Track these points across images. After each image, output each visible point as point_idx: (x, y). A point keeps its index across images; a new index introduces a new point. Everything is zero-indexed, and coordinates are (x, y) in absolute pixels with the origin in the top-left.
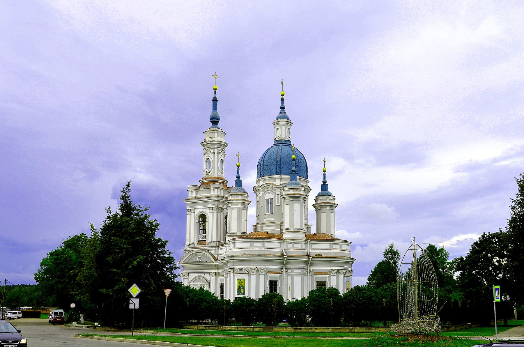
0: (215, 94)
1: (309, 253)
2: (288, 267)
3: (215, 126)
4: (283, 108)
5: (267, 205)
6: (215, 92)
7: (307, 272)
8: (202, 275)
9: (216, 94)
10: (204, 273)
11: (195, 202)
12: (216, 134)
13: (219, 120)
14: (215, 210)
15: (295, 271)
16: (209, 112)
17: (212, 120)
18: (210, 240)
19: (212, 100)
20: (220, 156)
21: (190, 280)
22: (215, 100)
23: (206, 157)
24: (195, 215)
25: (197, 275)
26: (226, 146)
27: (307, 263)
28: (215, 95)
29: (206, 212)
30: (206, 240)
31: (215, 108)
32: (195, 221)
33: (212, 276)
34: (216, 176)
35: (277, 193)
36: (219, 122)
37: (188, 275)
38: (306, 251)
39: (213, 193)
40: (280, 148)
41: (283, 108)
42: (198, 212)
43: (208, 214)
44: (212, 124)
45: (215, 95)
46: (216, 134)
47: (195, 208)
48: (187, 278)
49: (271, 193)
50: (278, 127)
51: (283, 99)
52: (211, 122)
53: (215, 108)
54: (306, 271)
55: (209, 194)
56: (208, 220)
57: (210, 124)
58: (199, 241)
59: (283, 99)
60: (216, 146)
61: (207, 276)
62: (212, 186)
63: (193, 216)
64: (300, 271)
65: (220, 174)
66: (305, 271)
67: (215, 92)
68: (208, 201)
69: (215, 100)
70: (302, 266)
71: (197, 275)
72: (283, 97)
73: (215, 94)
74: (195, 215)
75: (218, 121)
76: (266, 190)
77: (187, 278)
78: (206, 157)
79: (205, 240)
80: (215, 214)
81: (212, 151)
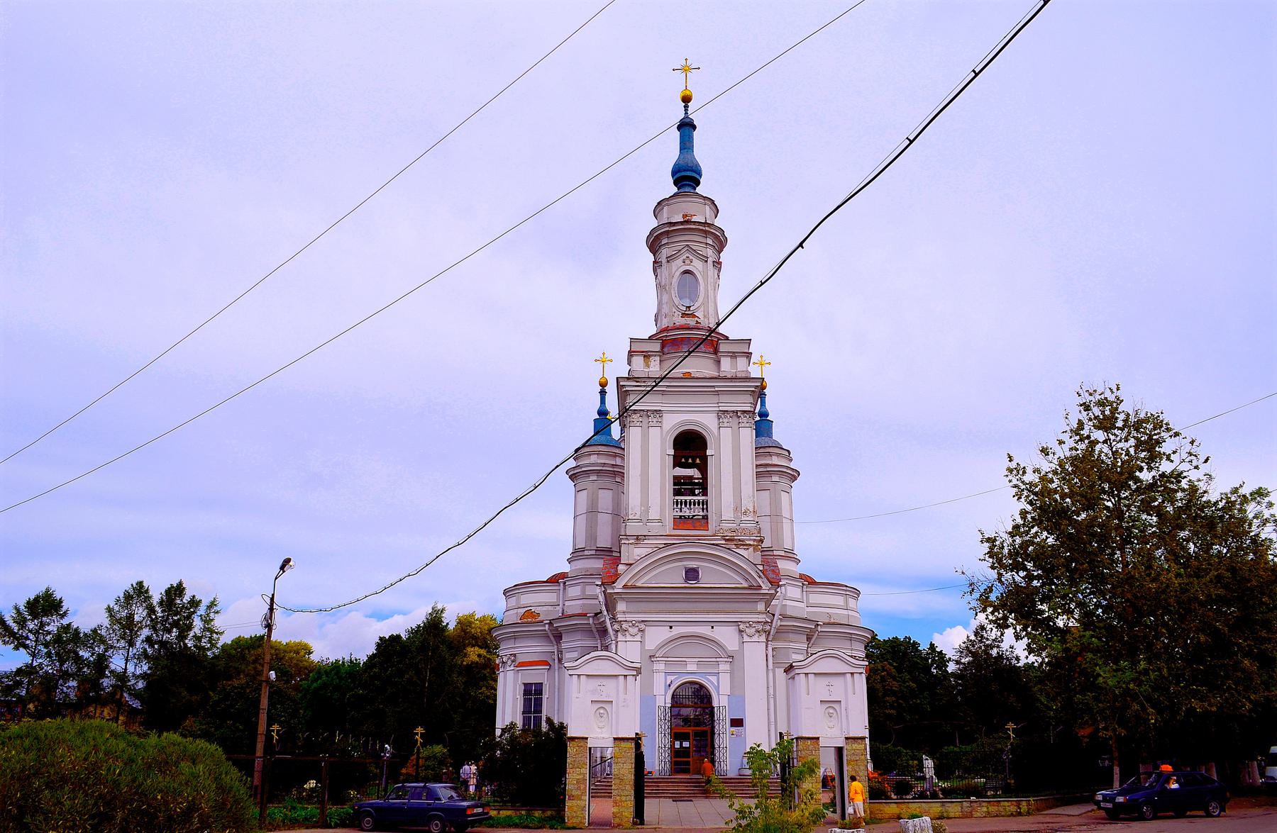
8: (704, 630)
10: (713, 624)
13: (700, 174)
16: (670, 152)
17: (679, 175)
18: (728, 514)
22: (686, 126)
24: (664, 433)
29: (705, 421)
31: (686, 144)
32: (663, 450)
33: (745, 636)
42: (674, 422)
45: (686, 113)
48: (638, 638)
53: (686, 144)
61: (727, 637)
68: (717, 389)
69: (686, 126)
71: (678, 630)
74: (664, 433)
77: (638, 638)
78: (678, 266)
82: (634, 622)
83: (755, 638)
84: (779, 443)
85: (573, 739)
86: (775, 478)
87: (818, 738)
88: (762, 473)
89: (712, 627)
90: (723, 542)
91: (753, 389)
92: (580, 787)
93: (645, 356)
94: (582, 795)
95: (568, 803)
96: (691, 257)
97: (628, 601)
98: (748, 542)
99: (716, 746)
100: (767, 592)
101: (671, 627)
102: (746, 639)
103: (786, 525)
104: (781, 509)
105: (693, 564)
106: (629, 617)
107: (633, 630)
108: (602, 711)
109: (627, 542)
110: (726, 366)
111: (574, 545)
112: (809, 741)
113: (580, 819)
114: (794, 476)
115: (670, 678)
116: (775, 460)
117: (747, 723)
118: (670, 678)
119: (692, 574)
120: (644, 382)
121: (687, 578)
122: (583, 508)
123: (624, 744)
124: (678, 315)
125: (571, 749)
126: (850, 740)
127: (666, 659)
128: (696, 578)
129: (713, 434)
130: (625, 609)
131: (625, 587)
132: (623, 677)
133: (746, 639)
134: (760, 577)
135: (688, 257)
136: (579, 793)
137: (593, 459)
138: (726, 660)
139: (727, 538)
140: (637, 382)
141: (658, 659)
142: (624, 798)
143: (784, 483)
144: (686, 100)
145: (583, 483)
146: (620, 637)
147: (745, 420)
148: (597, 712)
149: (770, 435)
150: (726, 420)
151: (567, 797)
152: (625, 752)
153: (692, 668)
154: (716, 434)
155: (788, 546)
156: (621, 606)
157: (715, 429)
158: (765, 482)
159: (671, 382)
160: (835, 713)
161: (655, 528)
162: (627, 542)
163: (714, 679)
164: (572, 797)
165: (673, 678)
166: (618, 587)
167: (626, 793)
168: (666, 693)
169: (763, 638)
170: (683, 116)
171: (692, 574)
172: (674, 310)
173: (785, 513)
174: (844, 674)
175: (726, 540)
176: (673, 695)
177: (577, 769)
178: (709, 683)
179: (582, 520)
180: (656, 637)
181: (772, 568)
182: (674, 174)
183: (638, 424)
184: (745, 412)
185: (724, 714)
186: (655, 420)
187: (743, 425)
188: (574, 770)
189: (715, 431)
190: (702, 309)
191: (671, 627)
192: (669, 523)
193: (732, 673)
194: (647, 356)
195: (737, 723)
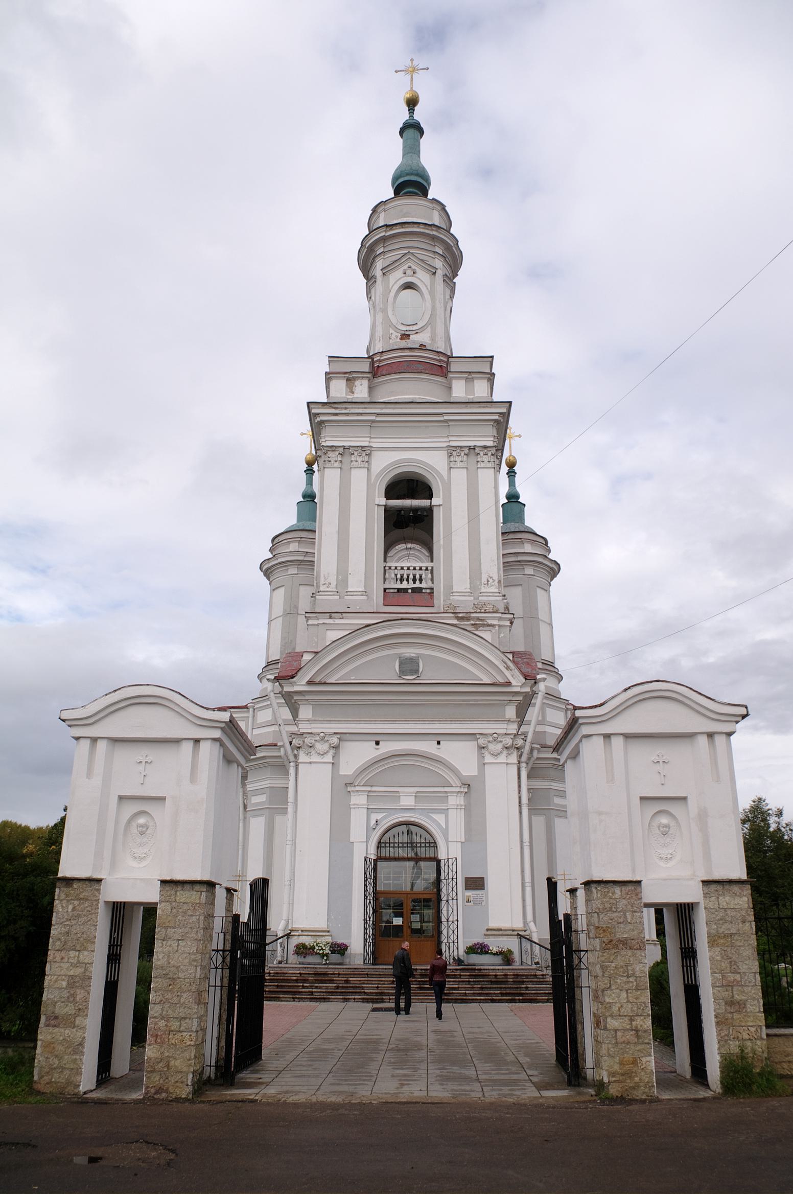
11: (373, 418)
18: (461, 583)
21: (348, 768)
24: (373, 477)
31: (412, 150)
37: (336, 748)
43: (444, 473)
48: (329, 758)
53: (412, 150)
63: (359, 477)
68: (446, 417)
71: (387, 747)
82: (322, 735)
83: (502, 758)
84: (533, 530)
85: (69, 881)
86: (529, 571)
87: (639, 883)
88: (511, 564)
89: (439, 743)
90: (455, 622)
91: (496, 417)
92: (73, 995)
93: (348, 380)
94: (76, 1016)
95: (44, 1034)
96: (414, 267)
97: (316, 706)
98: (490, 622)
99: (443, 919)
100: (518, 689)
101: (377, 743)
102: (488, 759)
103: (543, 628)
104: (537, 609)
105: (410, 652)
106: (317, 728)
107: (321, 747)
108: (142, 820)
109: (316, 622)
110: (459, 390)
111: (267, 657)
112: (617, 890)
113: (67, 1073)
114: (554, 570)
115: (375, 817)
116: (528, 548)
117: (490, 883)
118: (375, 817)
119: (409, 666)
120: (346, 408)
121: (403, 672)
122: (279, 610)
123: (183, 896)
124: (397, 337)
125: (62, 907)
126: (713, 887)
127: (369, 789)
128: (416, 671)
129: (441, 477)
130: (310, 717)
131: (310, 683)
132: (191, 744)
133: (488, 759)
134: (508, 668)
135: (410, 267)
136: (70, 1009)
137: (294, 547)
138: (458, 789)
139: (460, 615)
140: (336, 408)
141: (357, 788)
142: (174, 1025)
143: (541, 579)
145: (280, 576)
146: (302, 757)
147: (485, 458)
148: (134, 824)
149: (521, 518)
150: (458, 459)
151: (43, 1019)
152: (185, 913)
153: (407, 801)
154: (446, 478)
155: (546, 656)
156: (305, 712)
157: (443, 470)
158: (515, 576)
159: (382, 408)
160: (672, 824)
161: (357, 601)
162: (316, 622)
163: (440, 818)
164: (56, 1020)
165: (379, 816)
166: (300, 684)
167: (180, 1012)
168: (367, 842)
169: (514, 759)
171: (409, 666)
172: (391, 331)
173: (542, 615)
174: (691, 736)
175: (459, 619)
176: (380, 842)
177: (72, 954)
178: (434, 823)
179: (278, 624)
181: (525, 660)
183: (336, 464)
184: (485, 447)
185: (454, 870)
186: (360, 459)
187: (482, 465)
188: (63, 954)
189: (444, 473)
190: (429, 329)
191: (377, 743)
192: (378, 596)
193: (468, 809)
194: (350, 379)
195: (476, 883)
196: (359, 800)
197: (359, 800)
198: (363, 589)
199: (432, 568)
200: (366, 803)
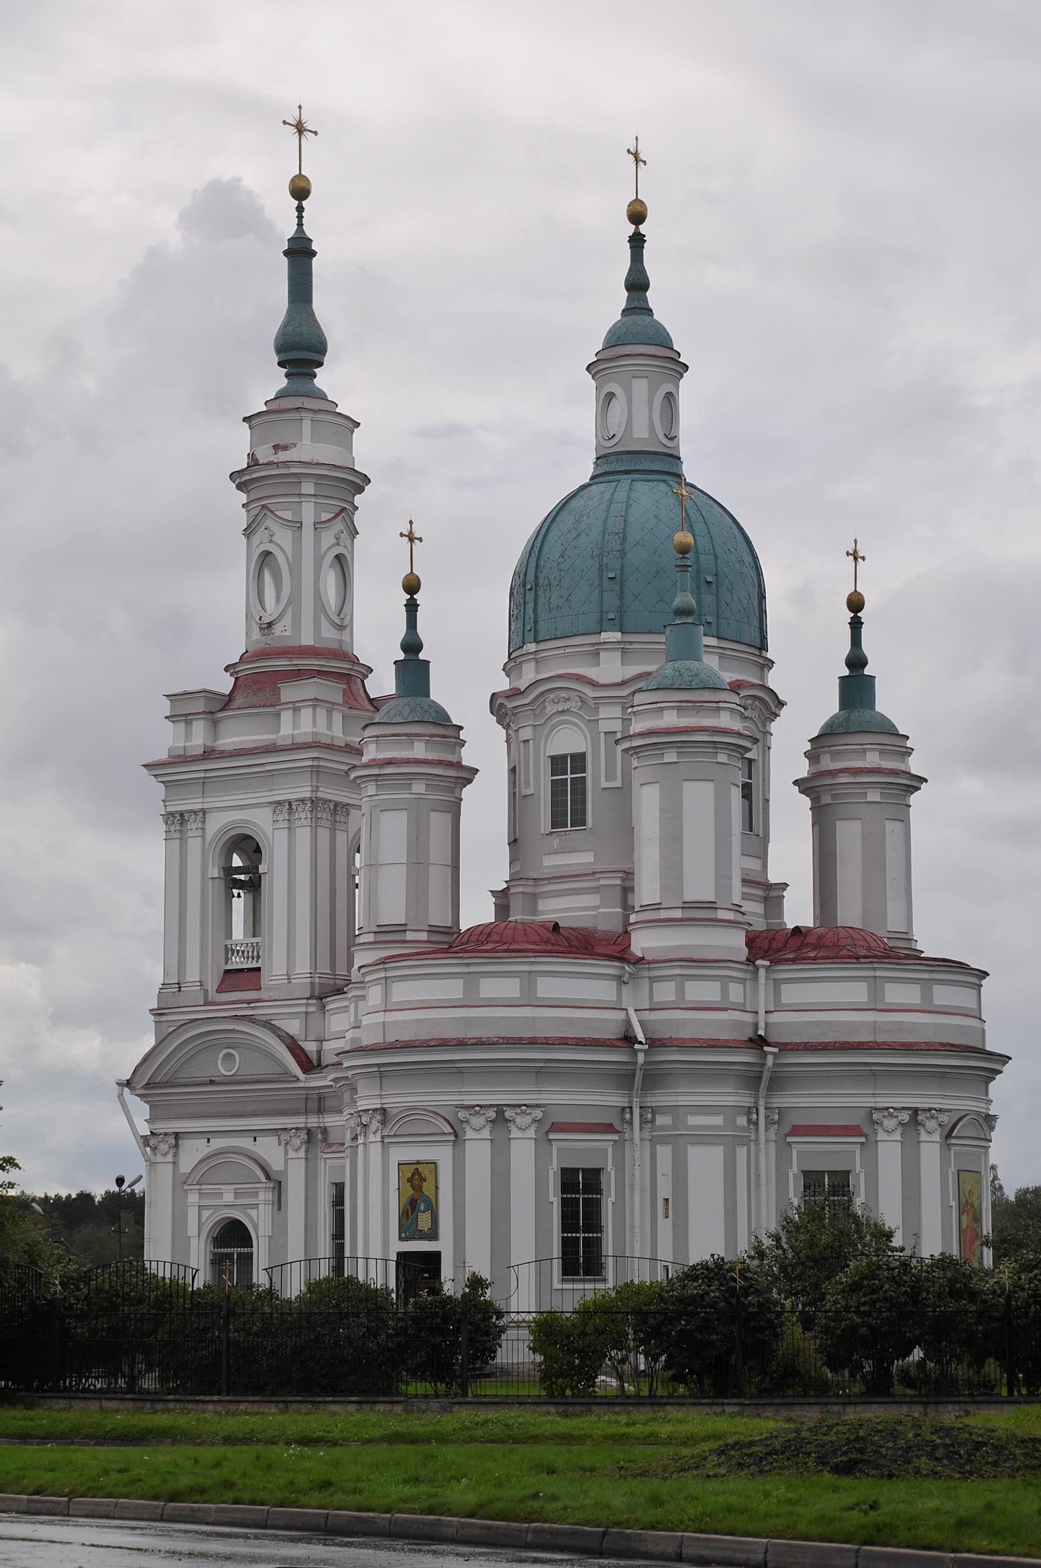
0: (300, 217)
1: (762, 1025)
2: (659, 1099)
3: (301, 384)
4: (637, 284)
5: (557, 788)
6: (300, 209)
7: (756, 1124)
8: (245, 1143)
9: (304, 221)
10: (255, 1134)
11: (202, 775)
12: (307, 425)
14: (304, 814)
15: (693, 1120)
19: (286, 253)
20: (328, 538)
21: (186, 1167)
23: (261, 542)
25: (218, 1143)
26: (361, 490)
27: (752, 1079)
28: (300, 224)
30: (258, 969)
34: (307, 639)
35: (604, 726)
36: (320, 364)
37: (176, 1146)
38: (748, 1018)
39: (289, 728)
40: (621, 494)
41: (637, 284)
42: (217, 823)
43: (270, 836)
44: (287, 376)
45: (300, 224)
46: (307, 425)
47: (206, 806)
48: (170, 1158)
49: (576, 725)
50: (613, 387)
51: (637, 241)
52: (281, 364)
54: (749, 1121)
55: (273, 737)
56: (271, 864)
57: (279, 379)
58: (227, 972)
59: (637, 241)
60: (308, 488)
61: (269, 1150)
62: (289, 692)
63: (194, 846)
64: (718, 1120)
65: (329, 633)
66: (742, 1121)
67: (300, 209)
68: (268, 768)
70: (731, 1096)
71: (218, 1143)
72: (643, 229)
73: (300, 217)
75: (315, 357)
76: (550, 709)
79: (254, 965)
80: (303, 835)
81: (287, 515)
127: (198, 1187)
133: (291, 1154)
144: (300, 191)
153: (228, 1198)
163: (253, 1213)
170: (290, 231)
180: (193, 1152)
182: (280, 349)
184: (303, 801)
196: (193, 1198)
197: (193, 1198)
198: (198, 979)
199: (226, 964)
200: (197, 1200)
